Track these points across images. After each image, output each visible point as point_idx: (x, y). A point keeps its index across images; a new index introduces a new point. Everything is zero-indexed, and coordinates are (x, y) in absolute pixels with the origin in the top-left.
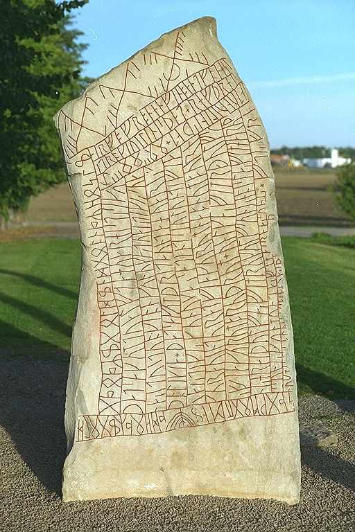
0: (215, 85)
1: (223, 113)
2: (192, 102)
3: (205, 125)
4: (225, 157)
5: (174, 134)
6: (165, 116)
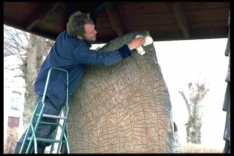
0: (138, 69)
1: (142, 87)
2: (124, 80)
3: (130, 94)
4: (142, 113)
5: (113, 99)
6: (109, 88)
